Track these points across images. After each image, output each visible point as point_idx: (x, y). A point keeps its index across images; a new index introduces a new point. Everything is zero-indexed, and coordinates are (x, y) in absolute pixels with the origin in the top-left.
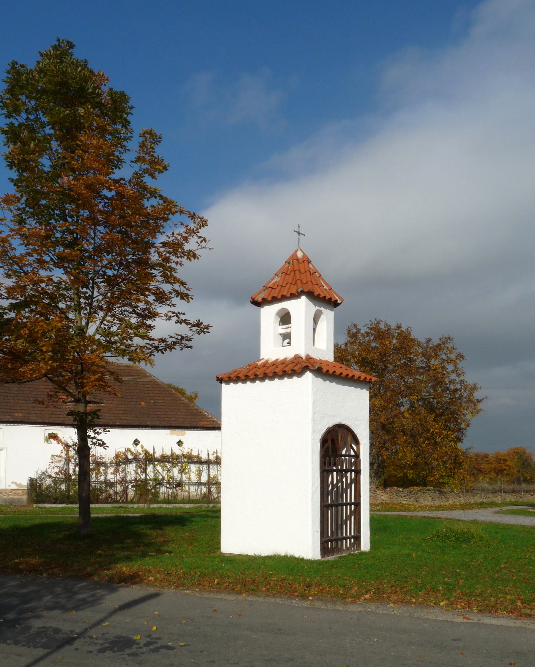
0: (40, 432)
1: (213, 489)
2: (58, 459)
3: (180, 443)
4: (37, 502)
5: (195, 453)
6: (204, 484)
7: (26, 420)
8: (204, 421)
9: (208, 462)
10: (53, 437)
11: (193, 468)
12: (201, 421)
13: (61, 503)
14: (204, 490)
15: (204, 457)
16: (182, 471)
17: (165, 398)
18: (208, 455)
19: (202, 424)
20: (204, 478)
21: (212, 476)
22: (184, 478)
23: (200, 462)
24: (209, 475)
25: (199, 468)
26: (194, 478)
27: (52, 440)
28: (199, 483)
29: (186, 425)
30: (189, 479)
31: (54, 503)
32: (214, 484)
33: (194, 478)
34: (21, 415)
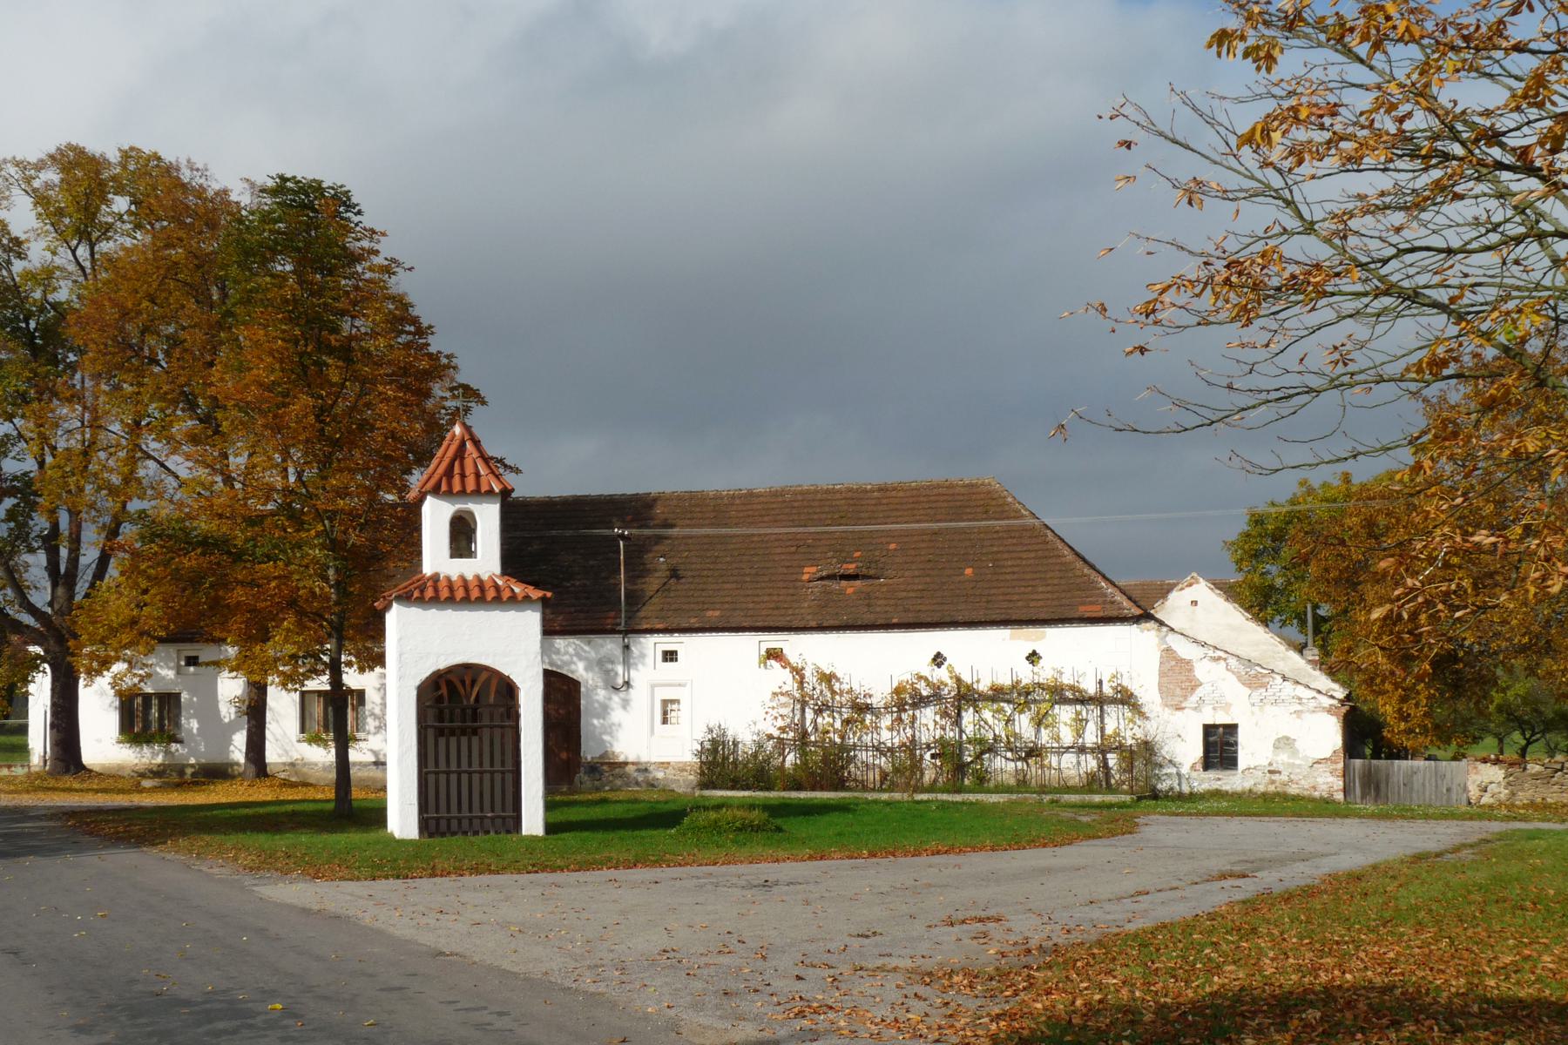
0: (749, 645)
1: (1112, 759)
2: (783, 699)
3: (1033, 657)
4: (704, 785)
5: (1067, 680)
6: (1092, 750)
7: (720, 625)
8: (1091, 603)
9: (1099, 701)
10: (774, 655)
11: (1065, 713)
12: (1083, 604)
13: (747, 788)
14: (1091, 763)
15: (1091, 689)
16: (1039, 722)
17: (1024, 555)
18: (1101, 682)
19: (1083, 610)
20: (1091, 737)
21: (1109, 731)
22: (1045, 737)
23: (1083, 700)
24: (1103, 729)
25: (1078, 713)
26: (1067, 737)
27: (773, 662)
28: (1082, 750)
29: (1043, 616)
30: (1058, 739)
31: (733, 788)
32: (1111, 750)
33: (1067, 737)
34: (717, 613)
